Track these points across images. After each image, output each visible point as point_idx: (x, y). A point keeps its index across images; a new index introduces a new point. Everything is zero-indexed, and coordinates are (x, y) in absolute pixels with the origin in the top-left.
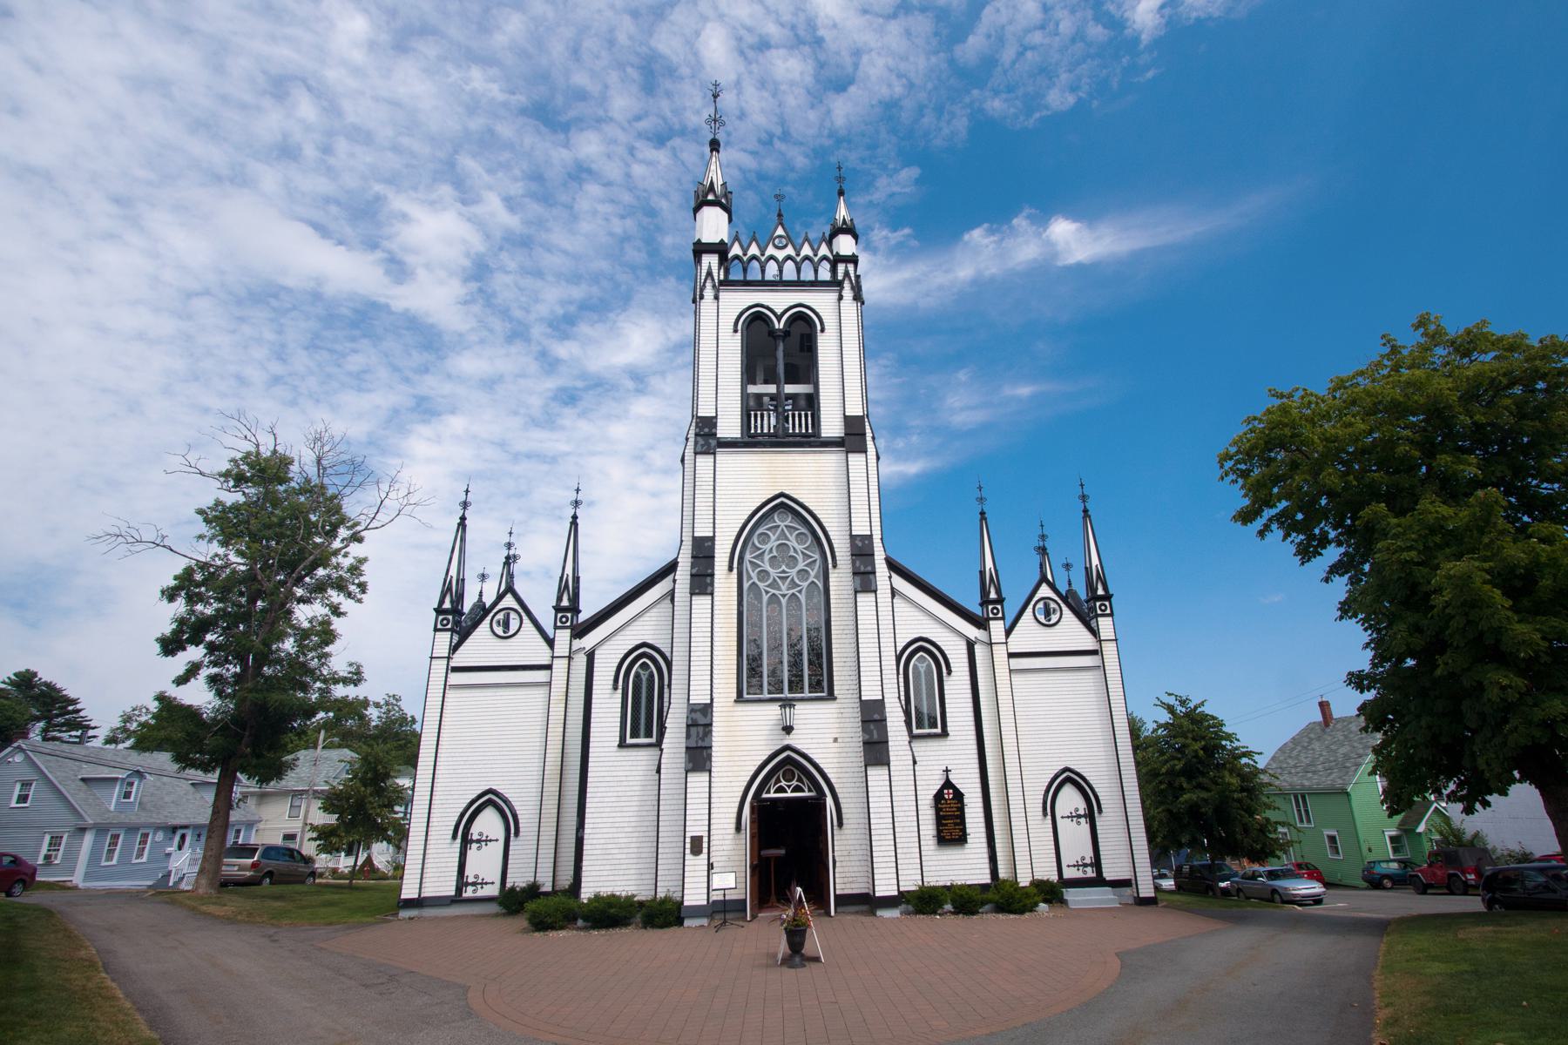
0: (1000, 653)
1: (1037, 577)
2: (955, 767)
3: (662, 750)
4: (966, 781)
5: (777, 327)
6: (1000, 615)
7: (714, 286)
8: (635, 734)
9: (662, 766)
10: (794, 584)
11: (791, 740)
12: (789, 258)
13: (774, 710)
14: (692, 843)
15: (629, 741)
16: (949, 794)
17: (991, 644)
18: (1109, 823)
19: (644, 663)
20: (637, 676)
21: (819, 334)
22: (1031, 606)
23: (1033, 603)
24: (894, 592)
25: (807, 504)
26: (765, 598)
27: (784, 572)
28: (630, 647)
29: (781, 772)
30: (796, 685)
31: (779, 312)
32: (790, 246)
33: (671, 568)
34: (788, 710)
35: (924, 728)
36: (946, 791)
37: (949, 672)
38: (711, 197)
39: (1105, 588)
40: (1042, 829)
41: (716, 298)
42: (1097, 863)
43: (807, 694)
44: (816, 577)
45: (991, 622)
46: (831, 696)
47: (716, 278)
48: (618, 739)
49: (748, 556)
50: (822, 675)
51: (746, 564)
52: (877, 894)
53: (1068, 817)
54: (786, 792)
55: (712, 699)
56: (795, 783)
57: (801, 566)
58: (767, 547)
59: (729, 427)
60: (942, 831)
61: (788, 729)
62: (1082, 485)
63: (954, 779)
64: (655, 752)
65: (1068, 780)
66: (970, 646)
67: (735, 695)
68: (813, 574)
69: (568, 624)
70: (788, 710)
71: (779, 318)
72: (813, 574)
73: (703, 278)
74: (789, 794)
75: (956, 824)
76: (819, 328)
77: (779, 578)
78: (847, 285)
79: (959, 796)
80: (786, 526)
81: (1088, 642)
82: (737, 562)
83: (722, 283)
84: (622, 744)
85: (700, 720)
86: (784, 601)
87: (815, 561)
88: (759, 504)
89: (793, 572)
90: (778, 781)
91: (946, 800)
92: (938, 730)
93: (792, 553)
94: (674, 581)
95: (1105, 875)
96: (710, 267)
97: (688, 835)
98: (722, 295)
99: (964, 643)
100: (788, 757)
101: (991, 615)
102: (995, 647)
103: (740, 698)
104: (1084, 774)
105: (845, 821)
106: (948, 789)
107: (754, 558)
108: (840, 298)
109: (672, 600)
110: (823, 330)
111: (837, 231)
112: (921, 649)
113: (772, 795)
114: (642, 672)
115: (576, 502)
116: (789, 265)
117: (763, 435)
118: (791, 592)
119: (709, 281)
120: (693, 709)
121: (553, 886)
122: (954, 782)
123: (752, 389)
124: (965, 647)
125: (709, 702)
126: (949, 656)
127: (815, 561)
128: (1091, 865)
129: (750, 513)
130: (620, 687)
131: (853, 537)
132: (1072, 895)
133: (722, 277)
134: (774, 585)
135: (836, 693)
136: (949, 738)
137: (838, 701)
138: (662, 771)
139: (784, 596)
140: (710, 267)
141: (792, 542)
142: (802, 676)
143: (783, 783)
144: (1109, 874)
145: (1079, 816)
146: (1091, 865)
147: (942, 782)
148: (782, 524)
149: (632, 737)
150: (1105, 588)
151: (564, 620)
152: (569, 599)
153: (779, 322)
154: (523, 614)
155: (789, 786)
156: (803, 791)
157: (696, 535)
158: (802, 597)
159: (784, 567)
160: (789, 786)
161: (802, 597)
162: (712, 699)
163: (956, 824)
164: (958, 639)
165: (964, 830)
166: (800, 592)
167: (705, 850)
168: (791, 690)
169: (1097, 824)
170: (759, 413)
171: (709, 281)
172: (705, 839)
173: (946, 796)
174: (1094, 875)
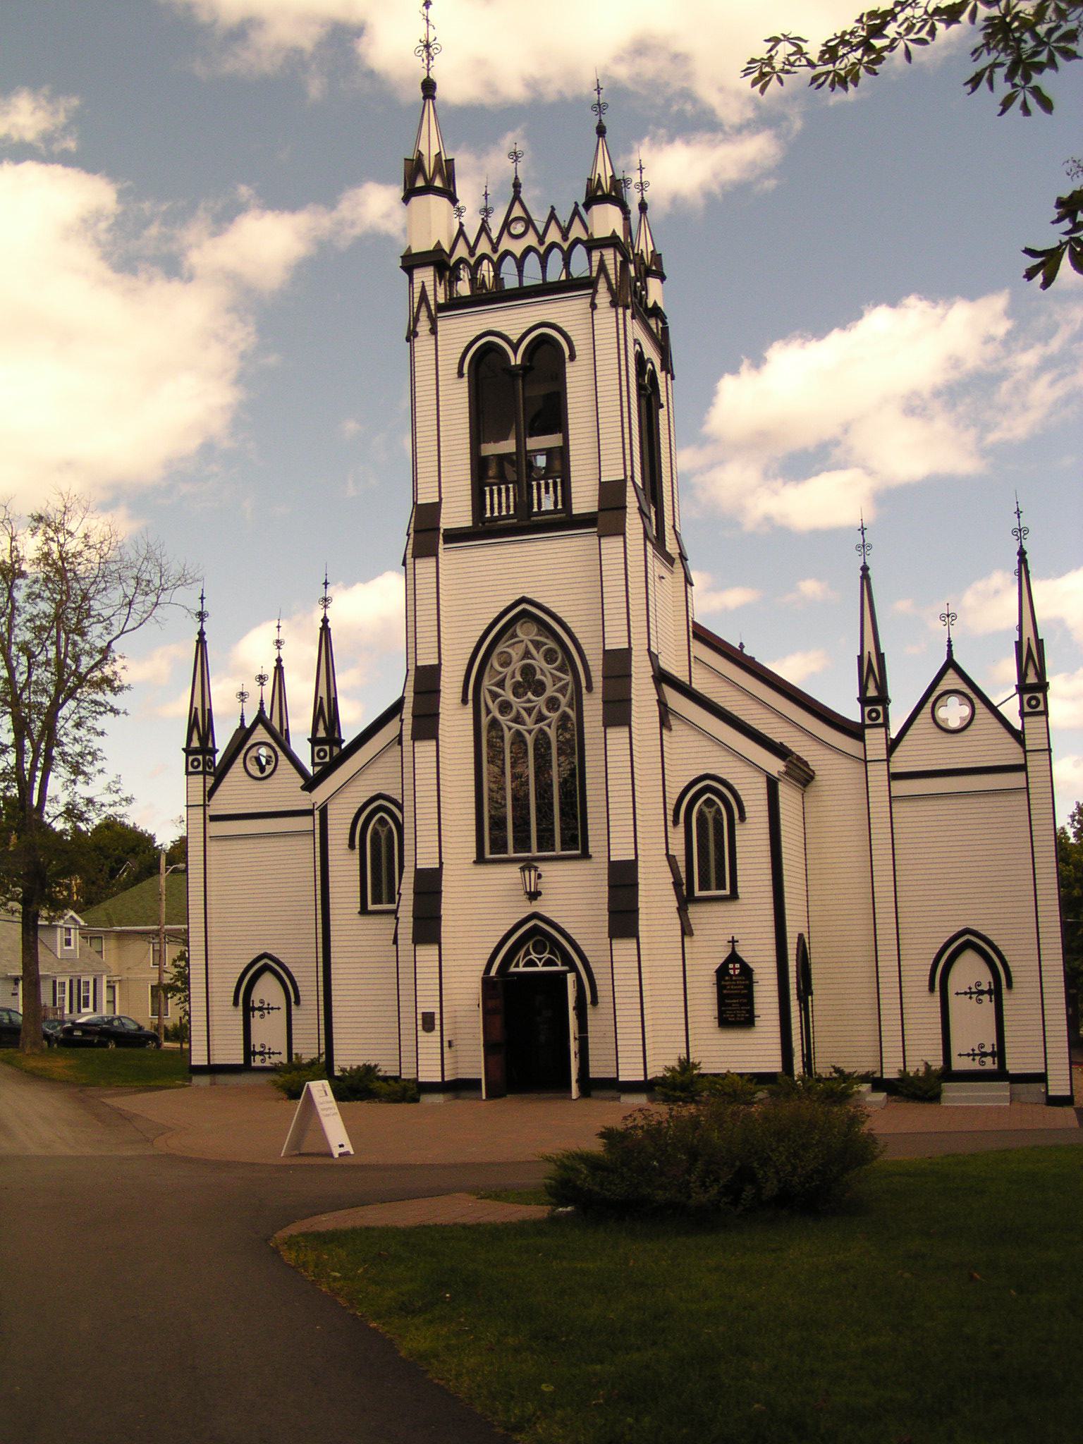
0: (878, 774)
1: (945, 658)
2: (744, 936)
3: (397, 919)
4: (758, 953)
5: (513, 363)
6: (880, 721)
9: (399, 937)
10: (541, 718)
11: (536, 907)
12: (529, 250)
13: (513, 871)
14: (423, 1019)
16: (734, 969)
17: (866, 762)
18: (1017, 1003)
19: (382, 818)
21: (567, 365)
22: (929, 705)
23: (932, 699)
24: (665, 716)
25: (553, 610)
26: (508, 735)
27: (529, 701)
28: (365, 800)
29: (530, 944)
30: (545, 841)
31: (515, 338)
32: (531, 231)
33: (396, 709)
34: (527, 873)
35: (708, 889)
36: (731, 966)
37: (743, 818)
38: (420, 183)
40: (925, 1009)
41: (434, 331)
42: (999, 1053)
43: (558, 852)
44: (570, 706)
45: (867, 731)
46: (586, 855)
47: (432, 302)
48: (359, 905)
49: (487, 683)
50: (577, 829)
51: (485, 696)
52: (621, 1079)
53: (966, 993)
55: (441, 863)
56: (546, 955)
58: (508, 670)
59: (457, 514)
61: (534, 895)
62: (1018, 513)
64: (391, 919)
65: (968, 945)
66: (772, 785)
67: (474, 856)
68: (564, 701)
69: (327, 759)
70: (527, 873)
71: (515, 348)
73: (416, 305)
74: (540, 968)
75: (742, 1004)
76: (567, 353)
77: (525, 709)
78: (602, 286)
79: (747, 971)
80: (532, 641)
82: (472, 693)
83: (441, 308)
84: (364, 911)
86: (530, 739)
88: (495, 615)
89: (540, 702)
90: (527, 953)
91: (731, 976)
92: (727, 892)
93: (539, 676)
94: (402, 720)
95: (1008, 1067)
96: (423, 287)
97: (420, 1011)
99: (765, 779)
100: (535, 927)
101: (868, 722)
103: (480, 860)
104: (991, 938)
105: (600, 1000)
106: (734, 963)
108: (593, 306)
109: (400, 743)
110: (573, 357)
111: (594, 197)
113: (521, 969)
114: (379, 828)
115: (278, 642)
116: (532, 261)
117: (501, 518)
118: (538, 726)
119: (424, 309)
121: (209, 1060)
122: (740, 954)
123: (490, 449)
124: (765, 785)
125: (437, 866)
126: (743, 798)
127: (567, 684)
128: (992, 1054)
129: (485, 627)
130: (357, 847)
131: (607, 654)
132: (953, 1093)
133: (441, 300)
134: (518, 719)
135: (591, 850)
136: (740, 901)
137: (593, 860)
138: (399, 942)
139: (530, 732)
140: (423, 287)
141: (539, 662)
142: (552, 830)
143: (534, 956)
144: (1013, 1067)
145: (981, 993)
146: (992, 1054)
147: (726, 955)
149: (374, 903)
151: (322, 754)
152: (325, 728)
153: (515, 353)
154: (278, 749)
156: (557, 965)
157: (419, 664)
158: (551, 733)
159: (530, 695)
160: (540, 960)
163: (742, 1004)
164: (756, 774)
167: (438, 1027)
168: (540, 849)
169: (1004, 1002)
170: (503, 487)
171: (424, 309)
172: (437, 1016)
173: (732, 972)
174: (996, 1067)
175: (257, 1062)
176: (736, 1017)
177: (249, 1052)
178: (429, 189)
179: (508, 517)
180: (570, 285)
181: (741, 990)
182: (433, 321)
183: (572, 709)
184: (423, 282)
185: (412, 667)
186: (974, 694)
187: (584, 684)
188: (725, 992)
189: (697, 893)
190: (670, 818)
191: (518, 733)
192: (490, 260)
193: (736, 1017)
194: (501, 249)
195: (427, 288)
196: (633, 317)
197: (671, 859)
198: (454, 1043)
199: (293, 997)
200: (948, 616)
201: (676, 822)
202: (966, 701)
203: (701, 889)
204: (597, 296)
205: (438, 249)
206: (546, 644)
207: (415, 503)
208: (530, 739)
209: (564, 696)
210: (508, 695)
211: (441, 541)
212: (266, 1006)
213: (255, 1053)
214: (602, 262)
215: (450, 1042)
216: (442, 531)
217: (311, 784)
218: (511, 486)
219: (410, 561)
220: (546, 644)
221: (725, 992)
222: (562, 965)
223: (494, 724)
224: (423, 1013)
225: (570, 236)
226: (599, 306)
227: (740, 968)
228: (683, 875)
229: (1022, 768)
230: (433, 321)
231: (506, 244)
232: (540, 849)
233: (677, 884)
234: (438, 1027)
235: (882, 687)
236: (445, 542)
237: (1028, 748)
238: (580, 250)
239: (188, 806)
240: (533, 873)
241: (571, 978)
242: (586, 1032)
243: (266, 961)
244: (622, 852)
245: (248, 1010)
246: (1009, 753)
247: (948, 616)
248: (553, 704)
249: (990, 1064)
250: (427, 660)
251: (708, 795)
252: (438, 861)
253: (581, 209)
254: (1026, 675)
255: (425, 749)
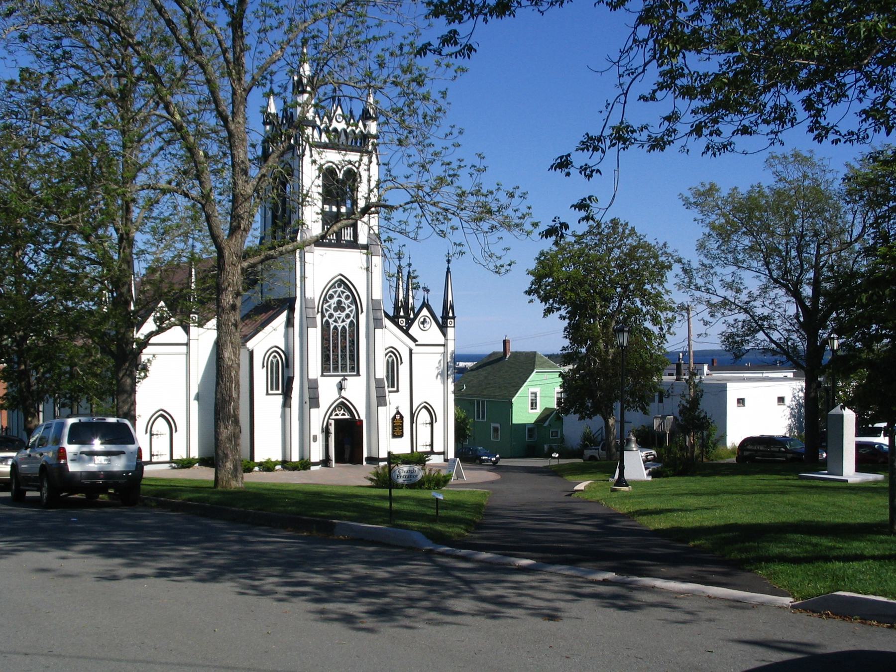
8: (272, 389)
15: (270, 392)
16: (398, 417)
18: (438, 427)
20: (272, 361)
26: (332, 327)
37: (402, 363)
39: (453, 313)
42: (432, 445)
46: (358, 374)
49: (325, 306)
57: (347, 311)
68: (352, 316)
72: (352, 316)
79: (402, 417)
81: (441, 340)
84: (268, 394)
85: (313, 387)
86: (340, 329)
89: (343, 315)
93: (343, 305)
134: (336, 321)
143: (338, 412)
150: (453, 313)
165: (402, 432)
175: (155, 459)
177: (152, 455)
191: (335, 326)
208: (340, 329)
213: (153, 455)
223: (327, 321)
232: (342, 371)
245: (151, 435)
248: (348, 316)
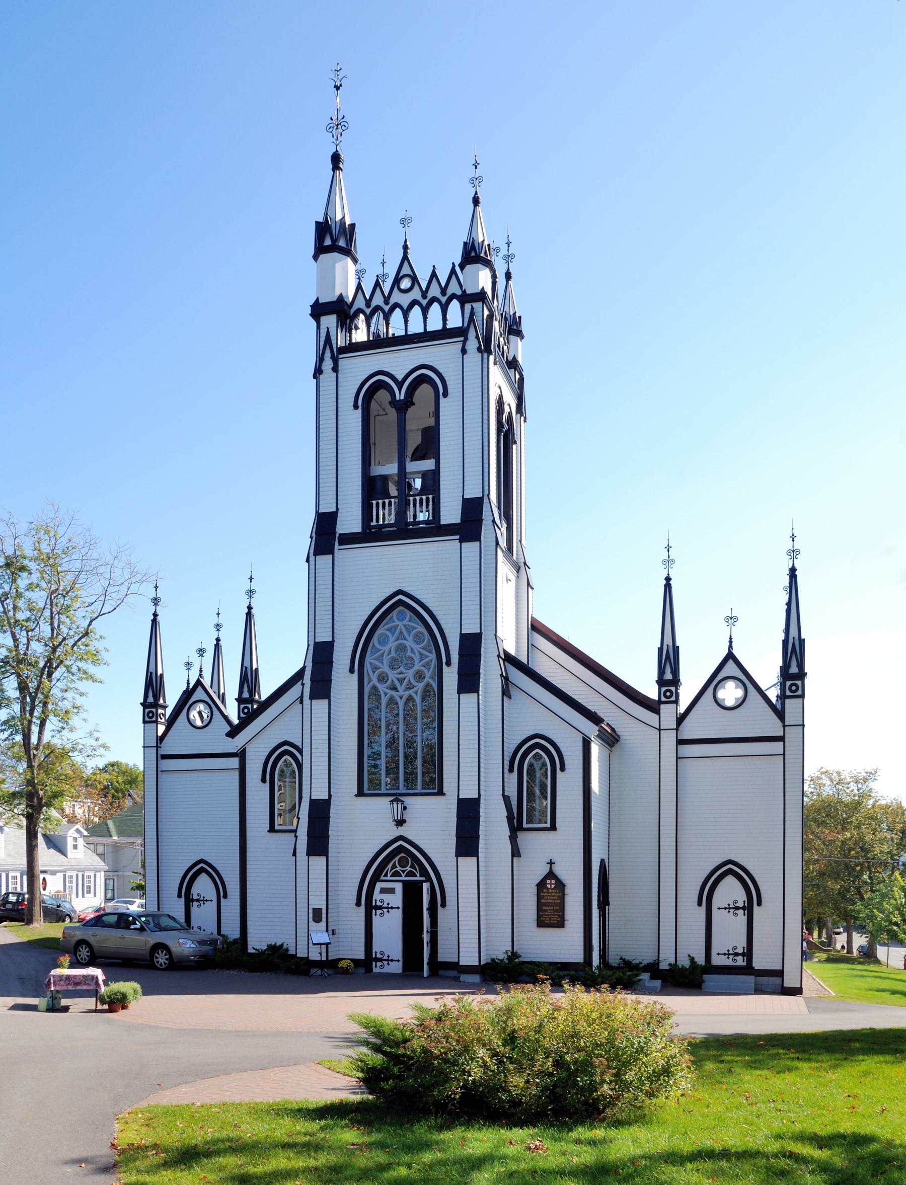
7: (333, 357)
11: (402, 831)
16: (551, 884)
26: (384, 701)
27: (401, 673)
36: (548, 881)
38: (328, 242)
41: (335, 369)
44: (432, 678)
46: (441, 793)
47: (334, 346)
49: (368, 659)
53: (725, 908)
54: (402, 876)
55: (330, 796)
56: (408, 868)
57: (417, 667)
58: (386, 649)
60: (542, 916)
61: (400, 822)
63: (557, 870)
65: (730, 872)
68: (428, 675)
72: (428, 675)
79: (561, 886)
82: (358, 665)
83: (342, 350)
87: (431, 661)
90: (394, 866)
93: (409, 654)
95: (754, 965)
96: (328, 332)
97: (311, 907)
98: (342, 363)
102: (661, 732)
103: (360, 793)
106: (551, 880)
107: (372, 659)
112: (537, 746)
117: (385, 526)
118: (407, 693)
120: (314, 803)
125: (327, 798)
127: (431, 661)
128: (743, 954)
140: (328, 332)
141: (410, 643)
143: (399, 869)
144: (758, 964)
145: (737, 908)
146: (743, 954)
148: (401, 624)
155: (403, 871)
156: (417, 876)
158: (418, 699)
160: (403, 871)
161: (418, 699)
162: (330, 796)
163: (556, 911)
166: (416, 693)
167: (324, 919)
172: (324, 912)
173: (549, 886)
174: (745, 964)
176: (550, 920)
178: (334, 248)
179: (390, 525)
180: (445, 334)
181: (556, 899)
182: (335, 361)
183: (434, 680)
184: (328, 328)
185: (312, 643)
186: (747, 680)
187: (444, 660)
188: (542, 901)
189: (525, 825)
190: (507, 767)
192: (383, 311)
193: (550, 920)
194: (392, 301)
195: (331, 333)
196: (495, 363)
197: (506, 799)
198: (337, 931)
199: (222, 892)
200: (731, 618)
201: (511, 770)
202: (740, 684)
203: (527, 823)
204: (468, 343)
205: (341, 298)
206: (416, 628)
207: (317, 512)
208: (401, 704)
209: (429, 669)
210: (385, 668)
211: (337, 543)
212: (202, 899)
214: (472, 313)
215: (333, 931)
216: (337, 535)
217: (234, 732)
218: (393, 500)
219: (312, 558)
220: (416, 628)
221: (542, 901)
222: (420, 876)
223: (375, 688)
224: (313, 909)
225: (447, 292)
226: (468, 351)
227: (555, 884)
228: (515, 811)
229: (781, 739)
230: (335, 361)
231: (396, 297)
233: (510, 818)
234: (324, 919)
235: (676, 672)
236: (340, 544)
237: (786, 724)
238: (455, 304)
239: (144, 747)
240: (400, 805)
241: (426, 886)
242: (437, 927)
243: (202, 865)
244: (468, 793)
246: (773, 727)
247: (731, 618)
248: (420, 676)
249: (740, 962)
250: (324, 636)
251: (537, 750)
252: (327, 794)
253: (458, 269)
254: (789, 666)
255: (321, 705)
